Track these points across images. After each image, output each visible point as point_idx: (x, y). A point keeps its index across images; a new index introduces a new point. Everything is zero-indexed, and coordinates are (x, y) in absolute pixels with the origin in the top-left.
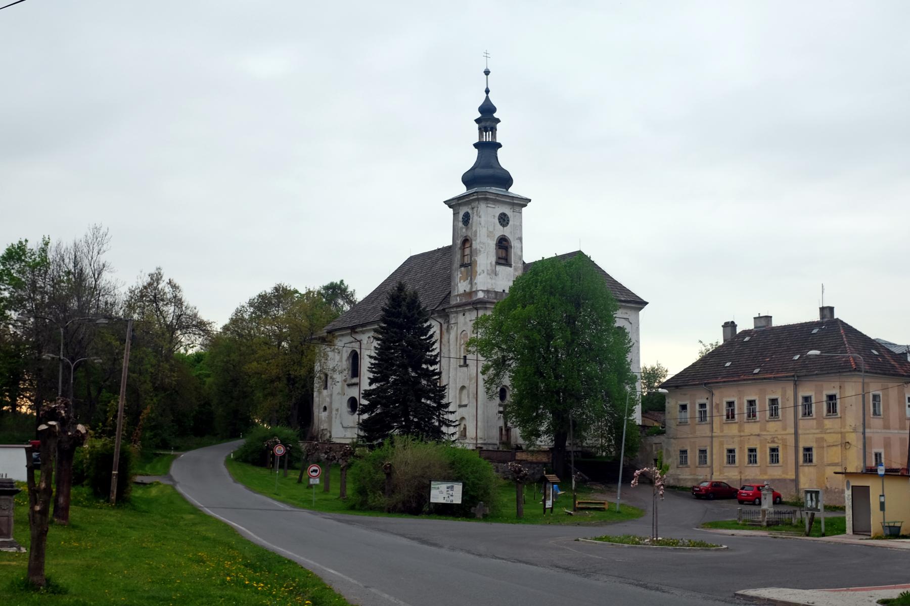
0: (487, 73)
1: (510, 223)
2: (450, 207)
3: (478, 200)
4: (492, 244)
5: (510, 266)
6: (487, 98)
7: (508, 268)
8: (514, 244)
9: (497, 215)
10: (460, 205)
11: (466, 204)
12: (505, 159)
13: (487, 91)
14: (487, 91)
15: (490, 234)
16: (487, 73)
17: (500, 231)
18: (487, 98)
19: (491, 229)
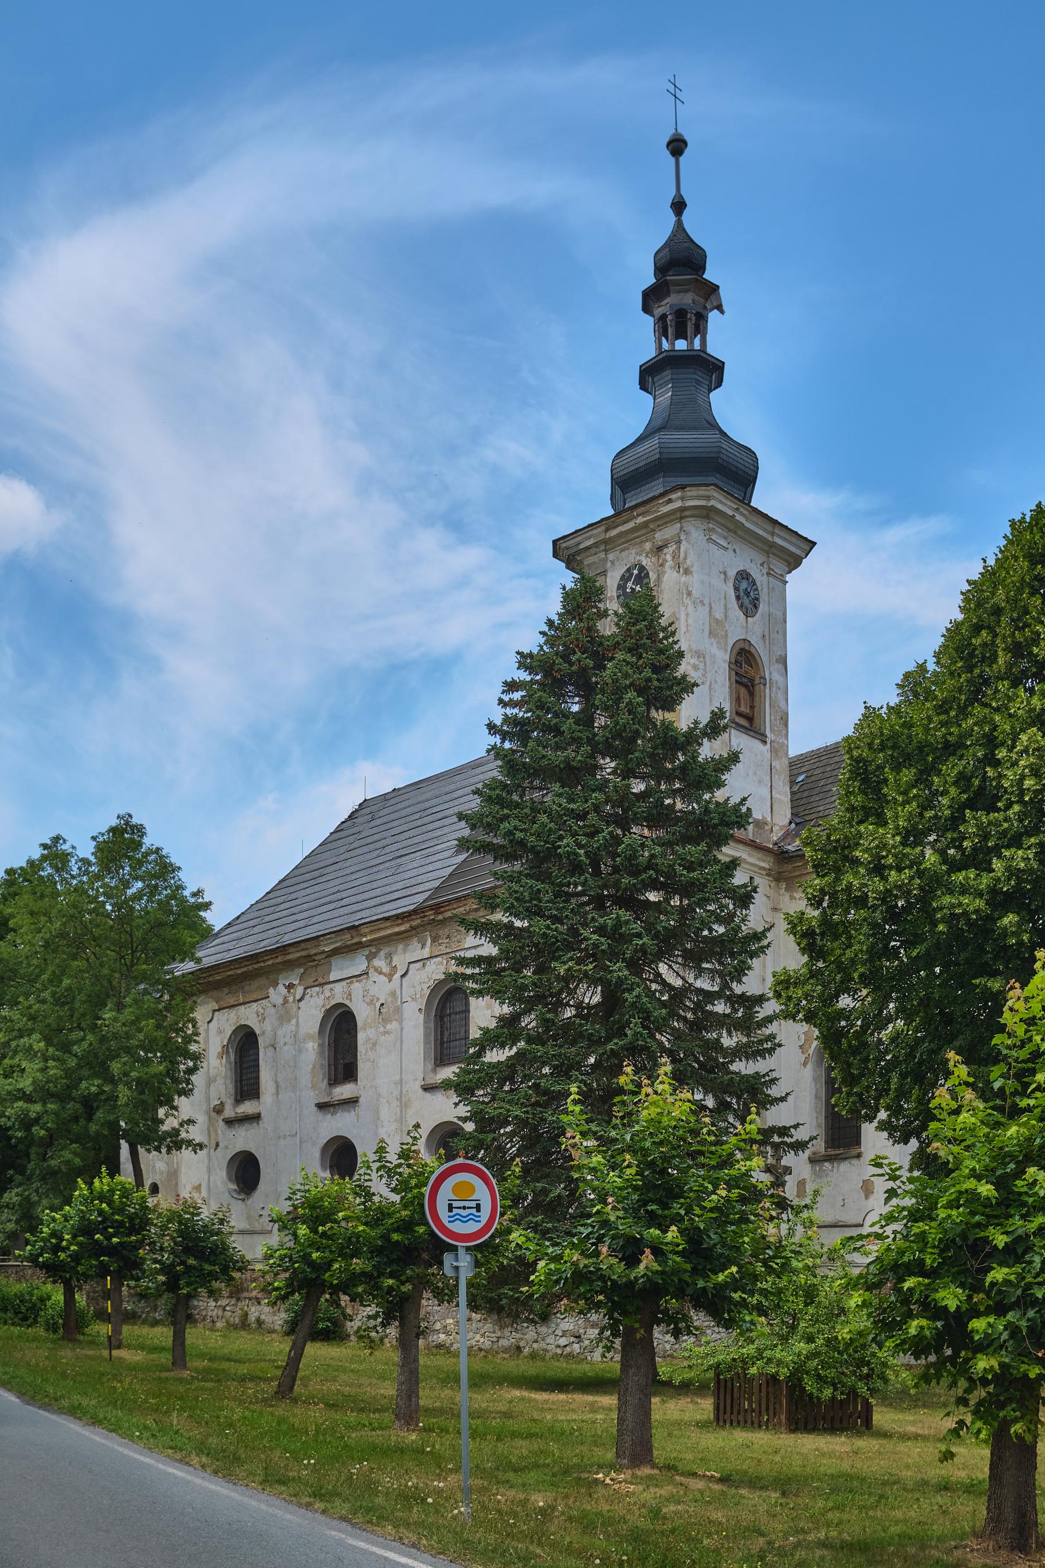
0: (677, 146)
1: (762, 607)
2: (571, 562)
3: (680, 515)
4: (721, 658)
5: (762, 738)
6: (679, 226)
7: (756, 744)
8: (771, 671)
9: (732, 573)
10: (608, 544)
11: (628, 539)
12: (736, 411)
13: (679, 206)
14: (679, 206)
15: (716, 629)
16: (677, 146)
17: (739, 627)
18: (679, 226)
19: (719, 615)
